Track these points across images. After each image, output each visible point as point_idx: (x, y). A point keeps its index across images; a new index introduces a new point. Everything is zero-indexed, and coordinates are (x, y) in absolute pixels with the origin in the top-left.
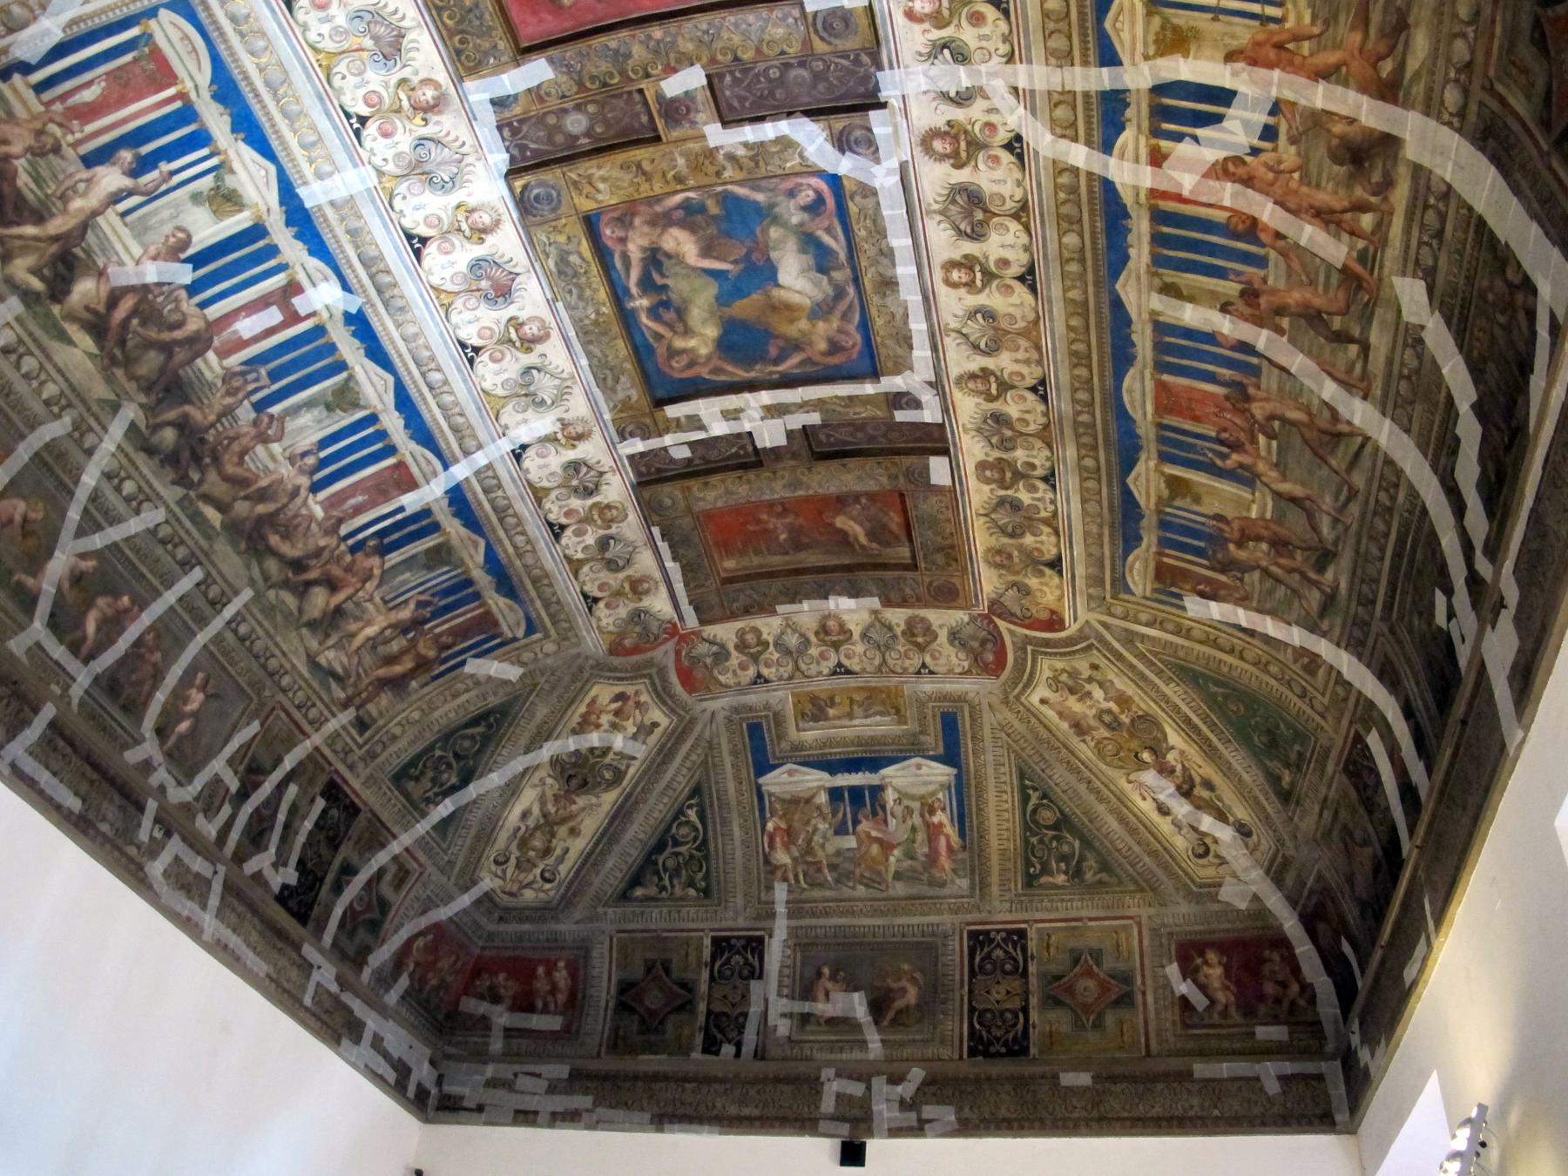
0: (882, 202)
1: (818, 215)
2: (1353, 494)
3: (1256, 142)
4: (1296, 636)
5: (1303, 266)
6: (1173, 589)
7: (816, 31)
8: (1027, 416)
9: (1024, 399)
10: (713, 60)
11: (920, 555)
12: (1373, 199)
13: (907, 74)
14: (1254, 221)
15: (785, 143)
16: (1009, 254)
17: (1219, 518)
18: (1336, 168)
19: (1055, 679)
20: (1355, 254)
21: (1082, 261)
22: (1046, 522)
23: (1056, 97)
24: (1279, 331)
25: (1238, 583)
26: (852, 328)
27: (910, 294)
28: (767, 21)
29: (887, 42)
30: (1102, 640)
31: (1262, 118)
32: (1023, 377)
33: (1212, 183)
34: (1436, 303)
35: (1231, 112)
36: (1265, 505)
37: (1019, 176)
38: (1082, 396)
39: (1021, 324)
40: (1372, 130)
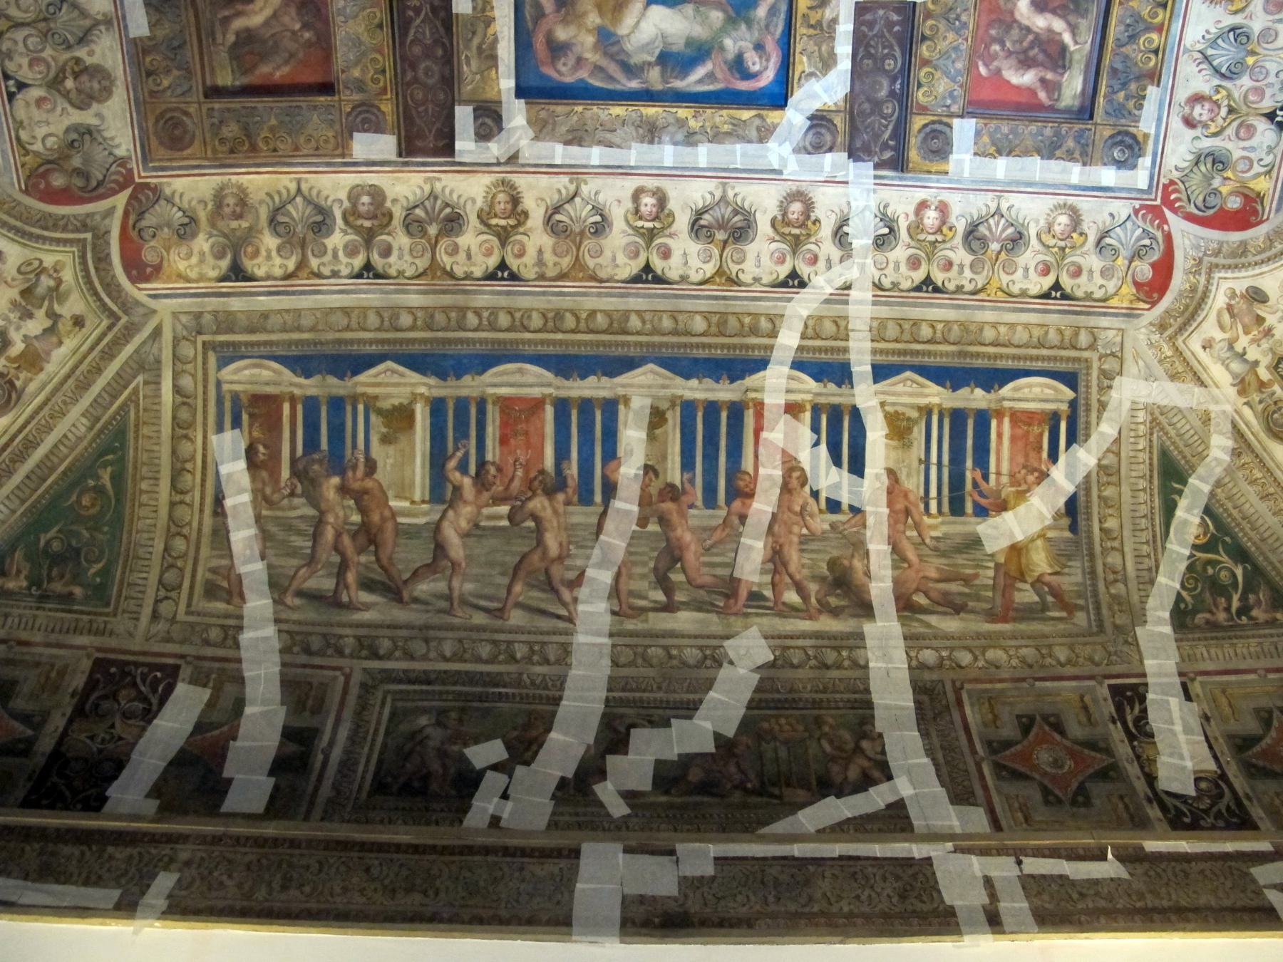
0: (749, 146)
1: (730, 69)
2: (499, 613)
3: (823, 495)
4: (251, 568)
5: (721, 542)
6: (245, 417)
7: (933, 122)
8: (462, 256)
9: (489, 253)
10: (929, 15)
11: (237, 103)
12: (813, 600)
13: (868, 191)
14: (750, 495)
15: (828, 62)
16: (676, 259)
17: (371, 467)
18: (824, 566)
19: (41, 270)
20: (755, 589)
21: (675, 332)
22: (302, 264)
23: (842, 323)
24: (643, 522)
25: (288, 491)
26: (583, 74)
27: (635, 154)
28: (954, 81)
29: (901, 179)
30: (130, 331)
31: (845, 500)
32: (521, 254)
33: (779, 457)
34: (766, 673)
35: (845, 473)
36: (415, 516)
37: (764, 281)
38: (504, 320)
39: (591, 263)
40: (869, 593)
